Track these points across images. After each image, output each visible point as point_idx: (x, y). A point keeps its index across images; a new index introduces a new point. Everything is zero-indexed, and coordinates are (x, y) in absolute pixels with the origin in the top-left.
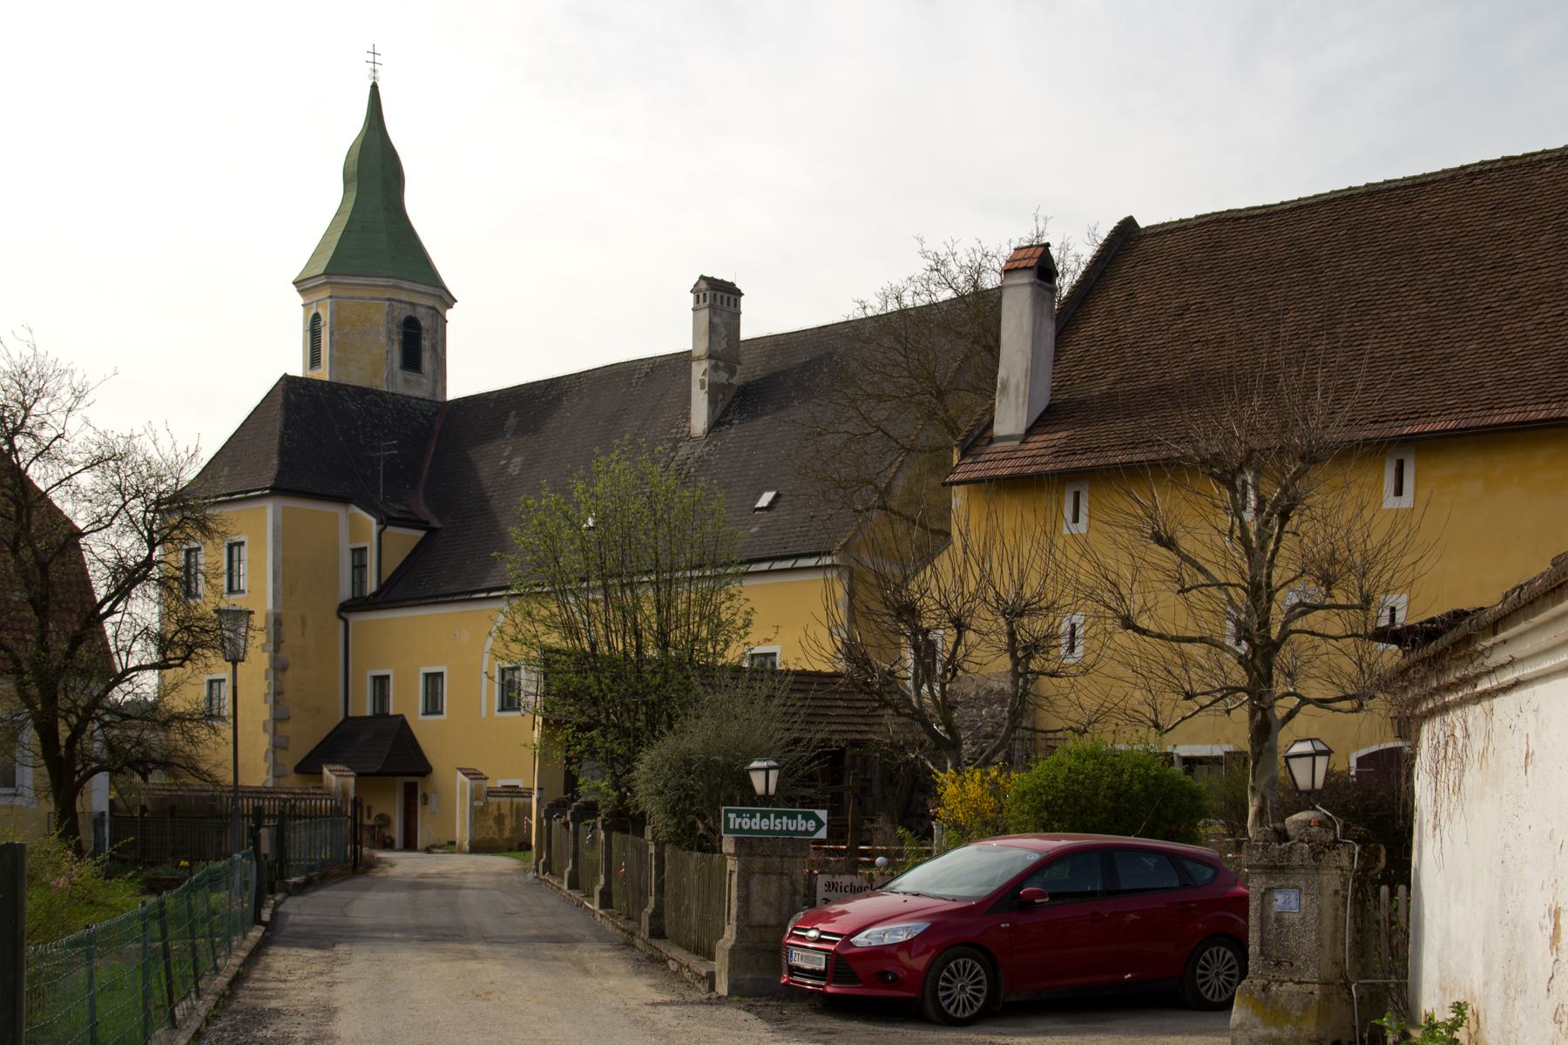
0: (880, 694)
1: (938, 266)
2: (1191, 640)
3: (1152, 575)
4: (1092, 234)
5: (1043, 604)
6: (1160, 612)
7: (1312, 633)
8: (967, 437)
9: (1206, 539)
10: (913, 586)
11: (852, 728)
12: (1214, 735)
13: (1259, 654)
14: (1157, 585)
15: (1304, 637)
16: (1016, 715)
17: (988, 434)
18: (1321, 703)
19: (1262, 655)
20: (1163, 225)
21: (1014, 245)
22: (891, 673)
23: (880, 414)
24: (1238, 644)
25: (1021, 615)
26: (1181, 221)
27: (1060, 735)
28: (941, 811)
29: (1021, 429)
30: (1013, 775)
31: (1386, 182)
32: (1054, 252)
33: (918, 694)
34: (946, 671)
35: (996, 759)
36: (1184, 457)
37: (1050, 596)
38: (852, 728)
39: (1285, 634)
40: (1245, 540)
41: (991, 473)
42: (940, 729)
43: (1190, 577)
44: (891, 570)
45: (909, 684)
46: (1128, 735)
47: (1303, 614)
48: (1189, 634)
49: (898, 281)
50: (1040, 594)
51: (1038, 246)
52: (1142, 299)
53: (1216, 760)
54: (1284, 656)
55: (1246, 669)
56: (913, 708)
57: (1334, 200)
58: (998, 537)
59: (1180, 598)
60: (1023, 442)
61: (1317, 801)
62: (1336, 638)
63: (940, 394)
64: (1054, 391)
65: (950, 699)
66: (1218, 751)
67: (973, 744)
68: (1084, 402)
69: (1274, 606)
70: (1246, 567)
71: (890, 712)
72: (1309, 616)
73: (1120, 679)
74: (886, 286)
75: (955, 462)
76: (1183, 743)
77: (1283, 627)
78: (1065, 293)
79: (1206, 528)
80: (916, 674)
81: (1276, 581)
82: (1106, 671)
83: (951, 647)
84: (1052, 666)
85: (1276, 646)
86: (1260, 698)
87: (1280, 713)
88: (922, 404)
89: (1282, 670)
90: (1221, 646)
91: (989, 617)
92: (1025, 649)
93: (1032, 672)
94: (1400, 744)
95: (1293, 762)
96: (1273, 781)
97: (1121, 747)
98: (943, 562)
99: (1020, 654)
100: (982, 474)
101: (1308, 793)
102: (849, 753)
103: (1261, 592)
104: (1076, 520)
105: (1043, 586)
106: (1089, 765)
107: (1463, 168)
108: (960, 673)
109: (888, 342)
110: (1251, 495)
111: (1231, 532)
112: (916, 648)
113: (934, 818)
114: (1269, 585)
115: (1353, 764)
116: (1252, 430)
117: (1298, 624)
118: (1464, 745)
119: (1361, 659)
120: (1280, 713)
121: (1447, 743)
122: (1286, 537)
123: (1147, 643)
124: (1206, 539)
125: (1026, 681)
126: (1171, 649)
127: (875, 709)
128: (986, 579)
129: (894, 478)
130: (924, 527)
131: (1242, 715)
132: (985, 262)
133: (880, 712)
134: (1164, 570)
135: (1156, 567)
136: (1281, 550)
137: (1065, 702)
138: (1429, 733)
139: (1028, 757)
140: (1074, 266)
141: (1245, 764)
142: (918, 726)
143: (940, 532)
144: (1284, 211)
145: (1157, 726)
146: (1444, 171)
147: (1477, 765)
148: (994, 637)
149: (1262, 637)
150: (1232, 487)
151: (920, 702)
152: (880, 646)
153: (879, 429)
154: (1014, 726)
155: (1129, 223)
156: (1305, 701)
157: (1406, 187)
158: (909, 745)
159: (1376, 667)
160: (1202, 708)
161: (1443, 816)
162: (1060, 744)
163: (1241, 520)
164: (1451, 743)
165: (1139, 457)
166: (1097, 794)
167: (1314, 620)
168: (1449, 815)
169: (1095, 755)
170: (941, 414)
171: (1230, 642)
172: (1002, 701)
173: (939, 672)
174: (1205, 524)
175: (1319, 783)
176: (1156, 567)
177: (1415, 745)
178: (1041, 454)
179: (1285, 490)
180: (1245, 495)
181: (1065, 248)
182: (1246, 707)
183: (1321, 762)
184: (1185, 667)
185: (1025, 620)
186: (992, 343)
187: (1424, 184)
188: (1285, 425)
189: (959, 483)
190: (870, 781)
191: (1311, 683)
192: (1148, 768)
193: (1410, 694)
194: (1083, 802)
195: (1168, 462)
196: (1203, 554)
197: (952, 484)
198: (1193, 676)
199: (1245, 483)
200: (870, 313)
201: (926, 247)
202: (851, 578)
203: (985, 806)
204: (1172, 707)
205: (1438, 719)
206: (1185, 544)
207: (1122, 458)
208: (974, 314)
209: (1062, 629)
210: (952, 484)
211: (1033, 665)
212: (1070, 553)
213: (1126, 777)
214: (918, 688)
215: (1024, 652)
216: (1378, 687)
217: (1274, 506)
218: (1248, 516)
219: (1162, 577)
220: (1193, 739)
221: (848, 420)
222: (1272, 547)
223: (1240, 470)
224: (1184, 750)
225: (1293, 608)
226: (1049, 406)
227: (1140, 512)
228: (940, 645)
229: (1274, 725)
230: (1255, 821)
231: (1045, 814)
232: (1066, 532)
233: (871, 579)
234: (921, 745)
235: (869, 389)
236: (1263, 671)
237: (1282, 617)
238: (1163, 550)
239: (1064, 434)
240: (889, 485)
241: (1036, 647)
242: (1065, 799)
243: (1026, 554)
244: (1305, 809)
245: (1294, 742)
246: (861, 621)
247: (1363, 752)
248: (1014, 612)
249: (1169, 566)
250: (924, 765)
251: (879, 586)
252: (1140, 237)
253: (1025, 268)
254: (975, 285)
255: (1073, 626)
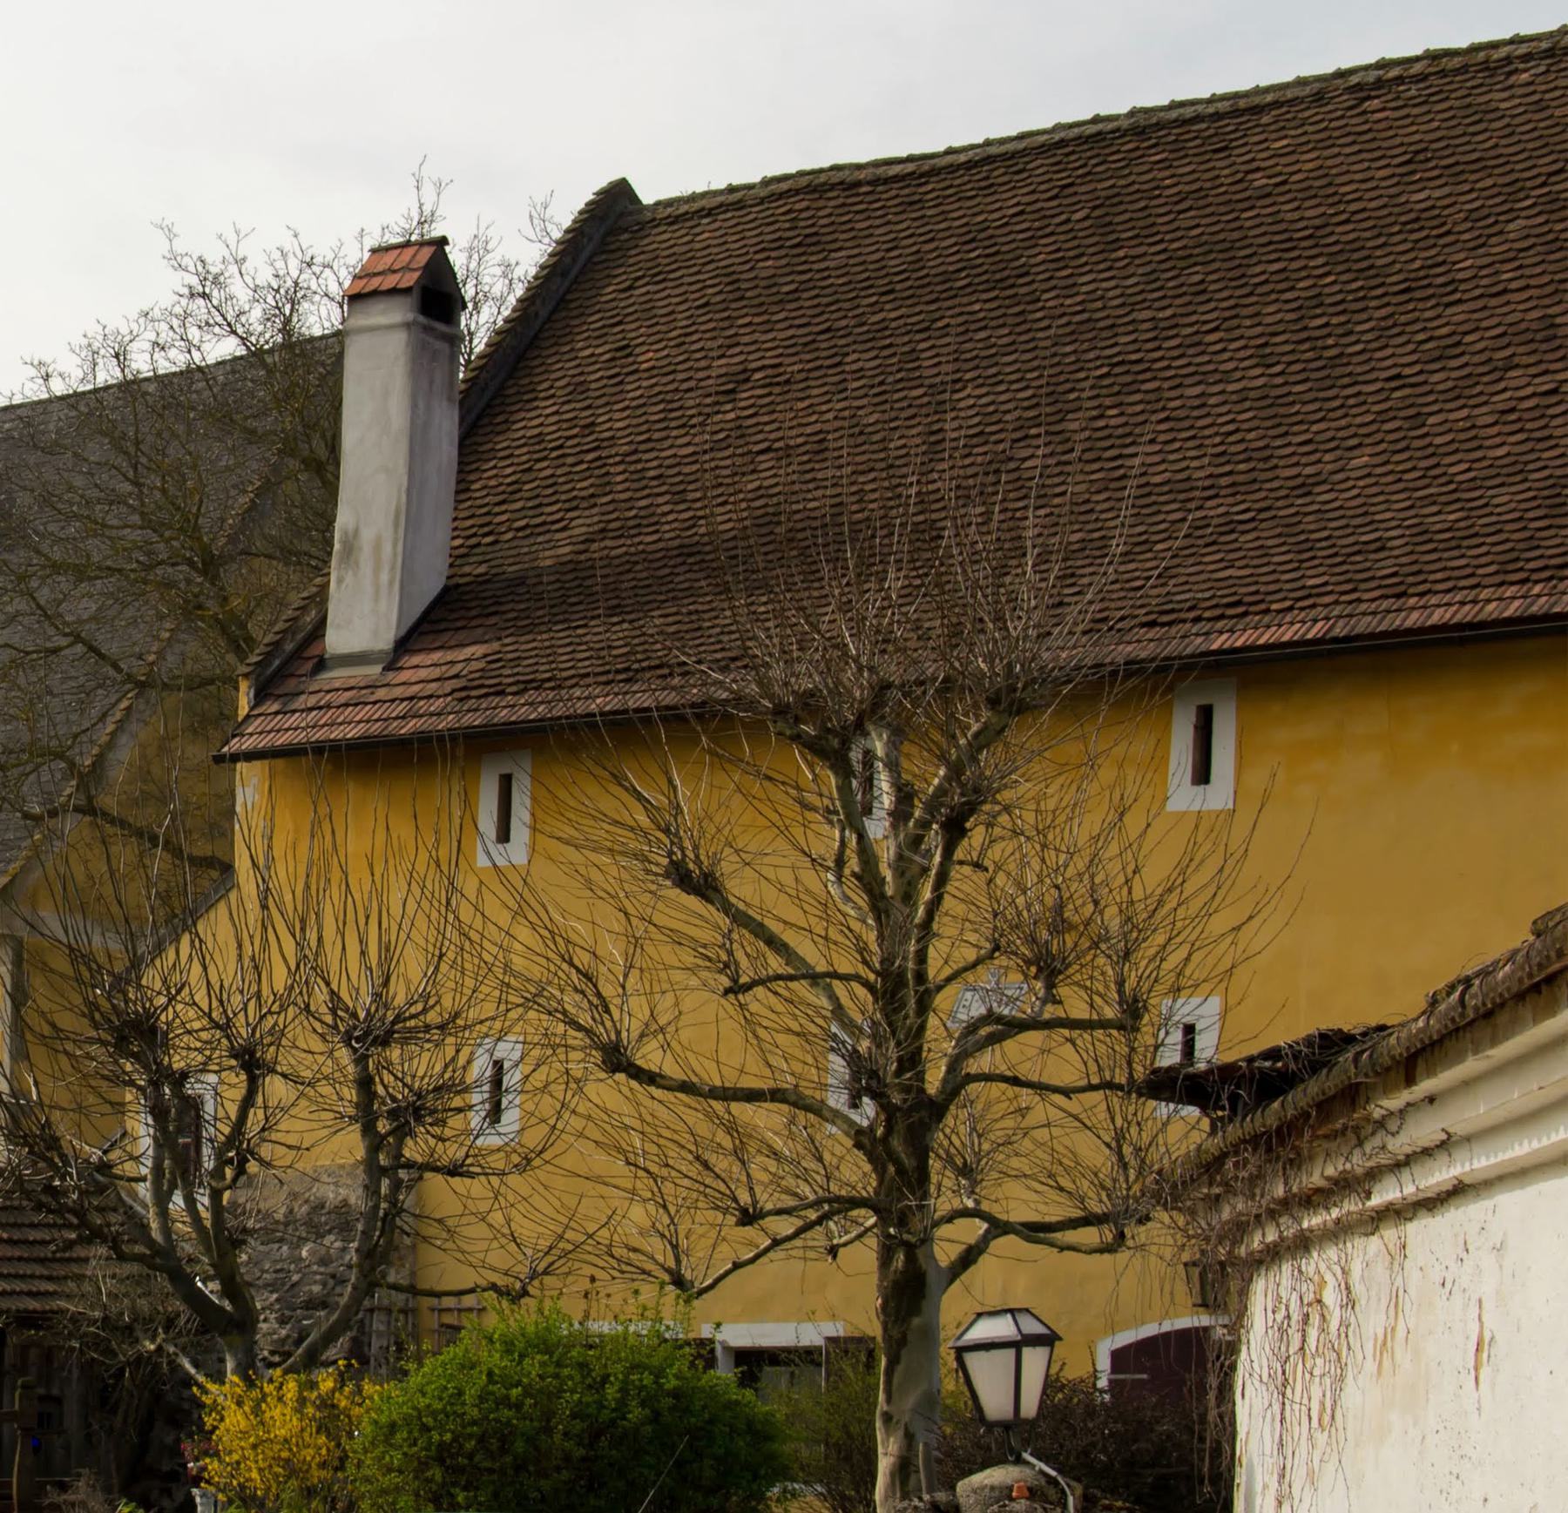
0: (80, 1212)
1: (206, 286)
2: (752, 1096)
3: (667, 953)
4: (539, 217)
5: (432, 1017)
6: (685, 1035)
7: (1015, 1081)
8: (268, 656)
9: (787, 877)
10: (152, 978)
11: (19, 1286)
12: (802, 1303)
13: (900, 1126)
14: (678, 976)
15: (997, 1088)
16: (374, 1258)
17: (313, 651)
18: (1035, 1231)
19: (907, 1128)
20: (693, 198)
21: (371, 242)
22: (105, 1167)
23: (82, 606)
24: (855, 1105)
25: (384, 1041)
26: (731, 189)
27: (468, 1301)
28: (213, 1465)
29: (385, 640)
30: (368, 1388)
31: (1174, 105)
32: (457, 257)
33: (164, 1214)
34: (222, 1162)
35: (331, 1353)
36: (738, 700)
37: (447, 1002)
38: (19, 1286)
39: (956, 1083)
40: (869, 880)
41: (319, 735)
42: (210, 1289)
43: (750, 959)
44: (106, 944)
45: (144, 1190)
46: (616, 1302)
47: (994, 1039)
48: (748, 1083)
49: (120, 320)
50: (425, 997)
51: (422, 244)
52: (646, 359)
53: (808, 1356)
54: (954, 1130)
55: (872, 1159)
56: (151, 1243)
57: (1062, 143)
58: (336, 875)
59: (729, 1004)
60: (390, 667)
61: (1026, 1444)
62: (1066, 1092)
63: (210, 565)
64: (457, 558)
65: (231, 1223)
66: (811, 1335)
67: (282, 1321)
68: (521, 581)
69: (933, 1021)
70: (871, 937)
71: (102, 1251)
72: (1009, 1044)
73: (599, 1180)
74: (94, 330)
75: (244, 707)
76: (736, 1319)
77: (952, 1068)
78: (480, 344)
79: (784, 852)
80: (158, 1170)
81: (935, 969)
82: (568, 1162)
83: (233, 1110)
84: (451, 1152)
85: (936, 1109)
86: (902, 1222)
87: (945, 1252)
88: (169, 584)
89: (949, 1160)
90: (818, 1110)
91: (317, 1045)
92: (393, 1114)
93: (410, 1165)
94: (1204, 1320)
95: (972, 1360)
96: (931, 1400)
97: (603, 1326)
98: (217, 927)
99: (383, 1126)
100: (301, 737)
101: (1006, 1426)
102: (13, 1340)
103: (901, 991)
104: (504, 836)
105: (433, 978)
106: (533, 1366)
107: (1341, 74)
108: (252, 1167)
109: (96, 450)
110: (883, 782)
111: (840, 862)
112: (158, 1112)
113: (197, 1481)
114: (921, 977)
115: (1104, 1363)
116: (884, 641)
117: (983, 1062)
118: (1344, 1324)
119: (1120, 1136)
120: (945, 1252)
121: (1306, 1319)
122: (956, 872)
123: (657, 1103)
124: (787, 877)
125: (397, 1185)
126: (711, 1116)
127: (70, 1245)
128: (310, 964)
129: (110, 745)
130: (175, 851)
131: (863, 1257)
132: (306, 278)
133: (79, 1252)
134: (696, 945)
135: (677, 939)
136: (948, 903)
137: (478, 1233)
138: (1268, 1298)
139: (400, 1348)
140: (499, 288)
141: (871, 1363)
142: (162, 1281)
143: (209, 862)
144: (953, 168)
145: (679, 1281)
146: (1301, 82)
147: (1370, 1366)
148: (325, 1089)
149: (906, 1089)
150: (841, 765)
151: (166, 1230)
152: (80, 1108)
153: (78, 639)
154: (370, 1282)
155: (617, 197)
156: (999, 1228)
157: (1218, 116)
158: (146, 1323)
159: (1153, 1155)
160: (776, 1243)
161: (1298, 1477)
162: (467, 1321)
163: (861, 836)
164: (1315, 1319)
165: (640, 698)
166: (548, 1430)
167: (1019, 1052)
168: (1312, 1478)
169: (544, 1344)
170: (213, 607)
171: (837, 1100)
172: (344, 1229)
173: (209, 1164)
174: (781, 844)
175: (1030, 1407)
176: (677, 939)
177: (1238, 1324)
178: (427, 694)
179: (956, 771)
180: (869, 783)
181: (481, 247)
182: (872, 1241)
183: (1035, 1362)
184: (739, 1154)
185: (394, 1053)
186: (322, 453)
187: (1257, 110)
188: (955, 631)
189: (250, 756)
190: (58, 1401)
191: (1014, 1188)
192: (659, 1374)
193: (1226, 1214)
194: (519, 1446)
195: (705, 712)
196: (778, 911)
197: (235, 758)
198: (759, 1175)
199: (869, 757)
200: (59, 388)
201: (179, 246)
202: (18, 962)
203: (308, 1454)
204: (712, 1242)
205: (1286, 1267)
206: (741, 887)
207: (602, 702)
208: (289, 385)
209: (475, 1072)
210: (235, 758)
211: (411, 1151)
212: (492, 907)
213: (611, 1392)
214: (162, 1199)
215: (393, 1124)
216: (1157, 1197)
217: (932, 806)
218: (877, 827)
219: (689, 959)
220: (756, 1311)
221: (12, 619)
222: (927, 894)
223: (859, 727)
224: (739, 1335)
225: (972, 1027)
226: (446, 590)
227: (643, 819)
228: (209, 1107)
229: (932, 1279)
230: (891, 1486)
231: (436, 1473)
232: (482, 861)
233: (61, 963)
234: (169, 1324)
235: (57, 554)
236: (909, 1162)
237: (949, 1047)
238: (692, 902)
239: (479, 650)
240: (99, 761)
241: (416, 1111)
242: (482, 1439)
243: (396, 911)
244: (1000, 1461)
245: (973, 1315)
246: (38, 1053)
247: (1125, 1338)
248: (371, 1036)
249: (706, 935)
250: (175, 1367)
251: (79, 979)
252: (642, 225)
253: (394, 291)
254: (286, 329)
255: (498, 1065)
